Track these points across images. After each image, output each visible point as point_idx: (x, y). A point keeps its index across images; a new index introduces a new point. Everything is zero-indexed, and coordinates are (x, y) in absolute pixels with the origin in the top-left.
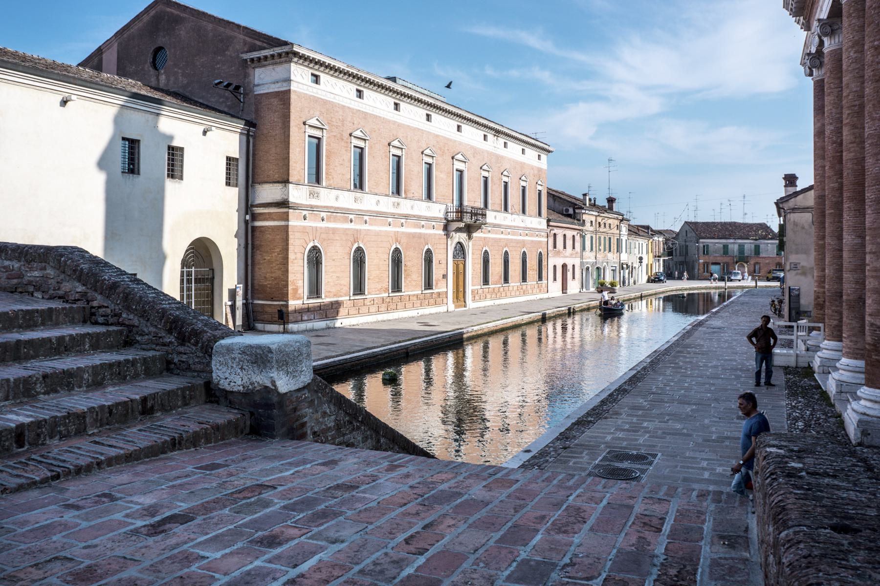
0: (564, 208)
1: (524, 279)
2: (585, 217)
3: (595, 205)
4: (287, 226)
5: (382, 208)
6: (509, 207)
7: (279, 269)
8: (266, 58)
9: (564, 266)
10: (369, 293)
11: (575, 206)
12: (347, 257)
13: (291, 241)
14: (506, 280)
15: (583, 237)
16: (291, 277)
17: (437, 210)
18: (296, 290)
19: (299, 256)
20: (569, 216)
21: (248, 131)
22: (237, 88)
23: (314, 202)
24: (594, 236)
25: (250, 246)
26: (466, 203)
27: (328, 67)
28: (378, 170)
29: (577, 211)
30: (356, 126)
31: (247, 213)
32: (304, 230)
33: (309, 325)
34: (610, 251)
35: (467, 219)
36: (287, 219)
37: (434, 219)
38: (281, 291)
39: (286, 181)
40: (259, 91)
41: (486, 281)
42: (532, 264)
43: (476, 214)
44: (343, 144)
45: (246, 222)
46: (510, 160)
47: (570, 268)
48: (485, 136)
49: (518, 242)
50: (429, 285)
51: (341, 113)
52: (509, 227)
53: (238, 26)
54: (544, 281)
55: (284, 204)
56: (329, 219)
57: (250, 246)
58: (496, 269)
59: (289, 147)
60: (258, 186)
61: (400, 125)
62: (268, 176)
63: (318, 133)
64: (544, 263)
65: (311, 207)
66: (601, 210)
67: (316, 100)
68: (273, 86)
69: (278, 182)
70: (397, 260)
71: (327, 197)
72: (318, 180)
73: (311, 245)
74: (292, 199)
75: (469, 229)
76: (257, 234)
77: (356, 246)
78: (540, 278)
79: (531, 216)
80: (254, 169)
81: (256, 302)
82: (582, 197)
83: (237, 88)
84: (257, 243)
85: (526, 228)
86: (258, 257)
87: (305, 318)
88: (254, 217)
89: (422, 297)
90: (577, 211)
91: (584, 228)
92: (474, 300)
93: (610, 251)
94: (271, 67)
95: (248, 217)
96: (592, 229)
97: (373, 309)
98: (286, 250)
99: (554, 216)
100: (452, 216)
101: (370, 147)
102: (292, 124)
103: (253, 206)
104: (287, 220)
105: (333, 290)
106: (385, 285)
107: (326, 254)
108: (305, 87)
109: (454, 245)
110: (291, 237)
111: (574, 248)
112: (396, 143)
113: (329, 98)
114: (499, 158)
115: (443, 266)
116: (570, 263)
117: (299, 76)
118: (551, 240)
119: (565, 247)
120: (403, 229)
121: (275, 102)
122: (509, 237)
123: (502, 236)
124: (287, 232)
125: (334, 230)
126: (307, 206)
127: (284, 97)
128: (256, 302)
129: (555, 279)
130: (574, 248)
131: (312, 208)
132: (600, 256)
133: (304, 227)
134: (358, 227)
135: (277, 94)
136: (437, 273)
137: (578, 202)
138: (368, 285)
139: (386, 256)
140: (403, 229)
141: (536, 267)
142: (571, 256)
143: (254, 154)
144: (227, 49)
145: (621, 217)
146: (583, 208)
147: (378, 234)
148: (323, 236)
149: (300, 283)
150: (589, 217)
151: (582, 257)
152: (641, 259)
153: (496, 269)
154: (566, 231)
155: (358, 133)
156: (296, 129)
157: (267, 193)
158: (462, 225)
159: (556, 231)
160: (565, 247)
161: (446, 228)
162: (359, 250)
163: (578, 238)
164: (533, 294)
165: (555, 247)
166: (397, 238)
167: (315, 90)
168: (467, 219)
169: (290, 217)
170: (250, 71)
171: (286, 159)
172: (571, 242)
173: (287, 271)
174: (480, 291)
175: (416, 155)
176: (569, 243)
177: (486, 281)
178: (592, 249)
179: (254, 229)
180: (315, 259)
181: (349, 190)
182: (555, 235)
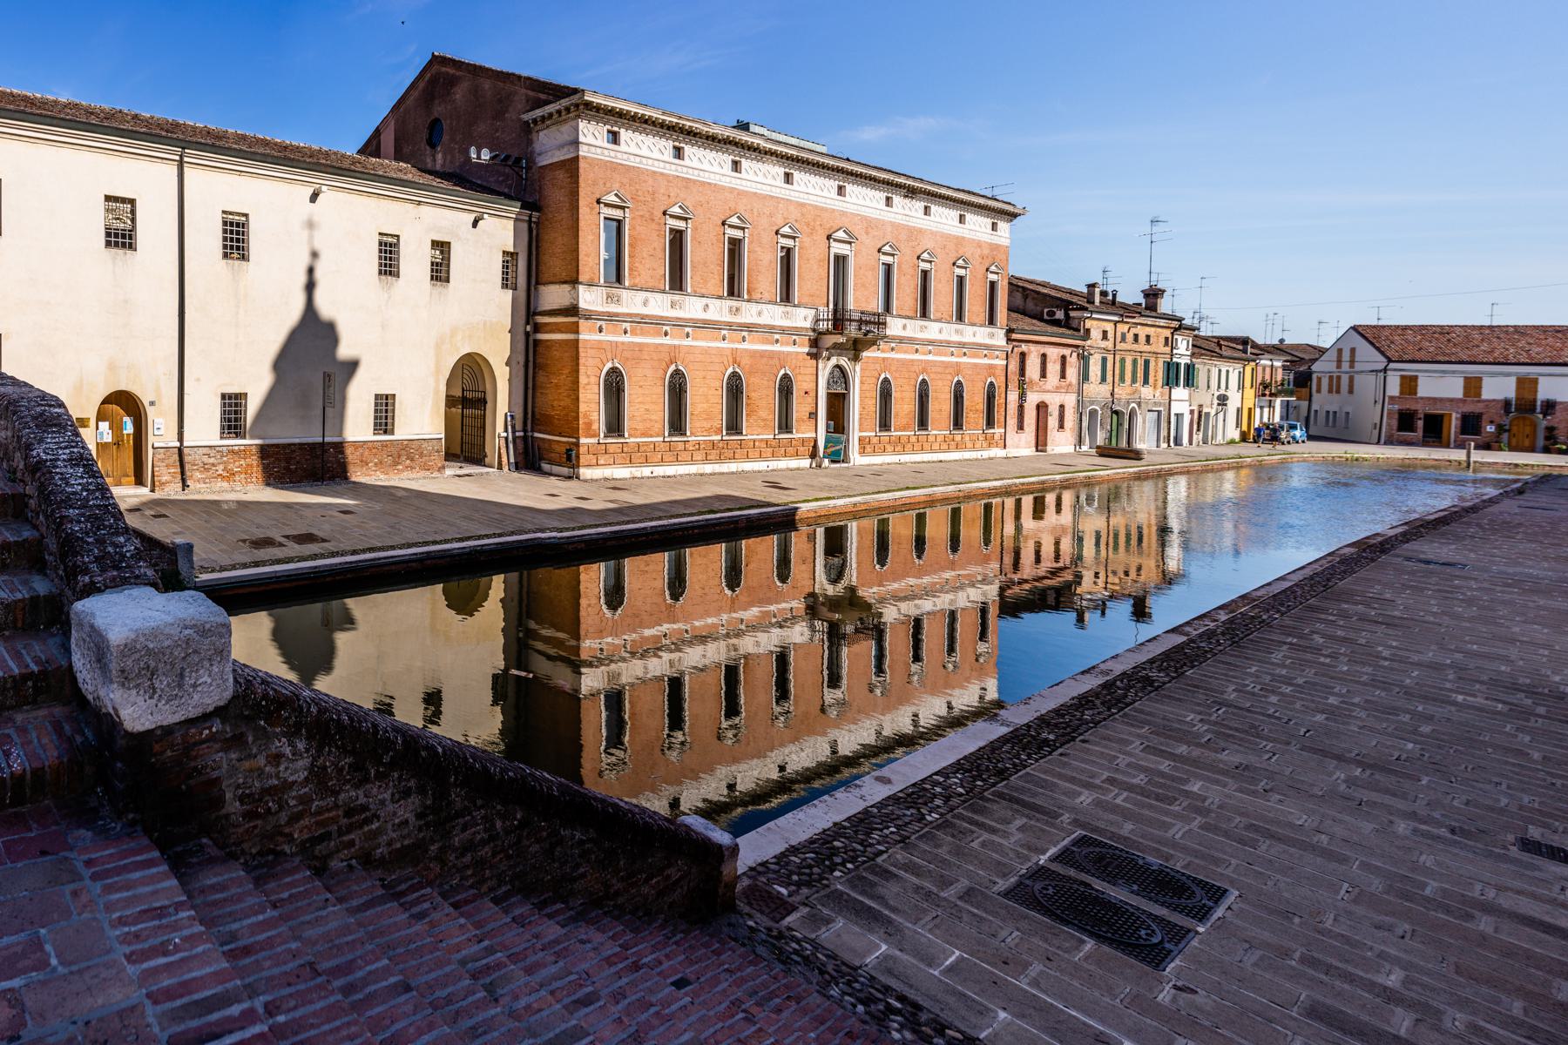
0: (1044, 309)
3: (1114, 302)
4: (577, 341)
5: (712, 315)
6: (932, 307)
9: (1042, 408)
11: (1066, 305)
12: (660, 383)
13: (582, 361)
15: (1084, 359)
16: (583, 408)
17: (801, 318)
19: (593, 380)
22: (518, 160)
24: (1110, 358)
28: (704, 257)
29: (1072, 314)
30: (673, 200)
32: (599, 346)
35: (852, 330)
36: (575, 329)
37: (796, 331)
39: (574, 281)
40: (544, 161)
43: (867, 323)
44: (654, 226)
45: (527, 334)
46: (932, 233)
51: (650, 182)
54: (998, 431)
56: (634, 333)
59: (577, 236)
60: (542, 288)
61: (741, 194)
63: (617, 214)
66: (1127, 311)
67: (614, 167)
68: (557, 153)
71: (632, 302)
73: (609, 365)
74: (582, 305)
75: (855, 348)
76: (540, 349)
77: (673, 368)
79: (973, 325)
80: (539, 264)
82: (1085, 290)
83: (518, 160)
84: (539, 360)
85: (962, 345)
86: (541, 378)
88: (537, 328)
89: (774, 443)
90: (1072, 314)
91: (1089, 342)
96: (1109, 344)
100: (823, 326)
101: (695, 229)
102: (582, 203)
103: (536, 314)
105: (640, 426)
106: (717, 424)
110: (582, 354)
111: (1063, 376)
113: (633, 162)
115: (810, 399)
116: (1053, 401)
117: (591, 135)
118: (1014, 366)
119: (1043, 375)
120: (745, 346)
121: (561, 175)
124: (577, 348)
126: (603, 313)
127: (571, 166)
130: (1063, 376)
131: (611, 317)
132: (1123, 392)
134: (676, 342)
137: (1075, 299)
138: (689, 424)
142: (1057, 390)
145: (1175, 324)
148: (626, 354)
149: (594, 416)
150: (1096, 326)
151: (1080, 392)
154: (1043, 350)
155: (676, 210)
157: (553, 296)
158: (841, 339)
159: (1024, 347)
160: (1043, 375)
161: (814, 343)
162: (677, 373)
166: (735, 358)
168: (852, 330)
171: (575, 251)
172: (1058, 367)
174: (875, 440)
176: (1053, 368)
181: (663, 292)
182: (1023, 355)
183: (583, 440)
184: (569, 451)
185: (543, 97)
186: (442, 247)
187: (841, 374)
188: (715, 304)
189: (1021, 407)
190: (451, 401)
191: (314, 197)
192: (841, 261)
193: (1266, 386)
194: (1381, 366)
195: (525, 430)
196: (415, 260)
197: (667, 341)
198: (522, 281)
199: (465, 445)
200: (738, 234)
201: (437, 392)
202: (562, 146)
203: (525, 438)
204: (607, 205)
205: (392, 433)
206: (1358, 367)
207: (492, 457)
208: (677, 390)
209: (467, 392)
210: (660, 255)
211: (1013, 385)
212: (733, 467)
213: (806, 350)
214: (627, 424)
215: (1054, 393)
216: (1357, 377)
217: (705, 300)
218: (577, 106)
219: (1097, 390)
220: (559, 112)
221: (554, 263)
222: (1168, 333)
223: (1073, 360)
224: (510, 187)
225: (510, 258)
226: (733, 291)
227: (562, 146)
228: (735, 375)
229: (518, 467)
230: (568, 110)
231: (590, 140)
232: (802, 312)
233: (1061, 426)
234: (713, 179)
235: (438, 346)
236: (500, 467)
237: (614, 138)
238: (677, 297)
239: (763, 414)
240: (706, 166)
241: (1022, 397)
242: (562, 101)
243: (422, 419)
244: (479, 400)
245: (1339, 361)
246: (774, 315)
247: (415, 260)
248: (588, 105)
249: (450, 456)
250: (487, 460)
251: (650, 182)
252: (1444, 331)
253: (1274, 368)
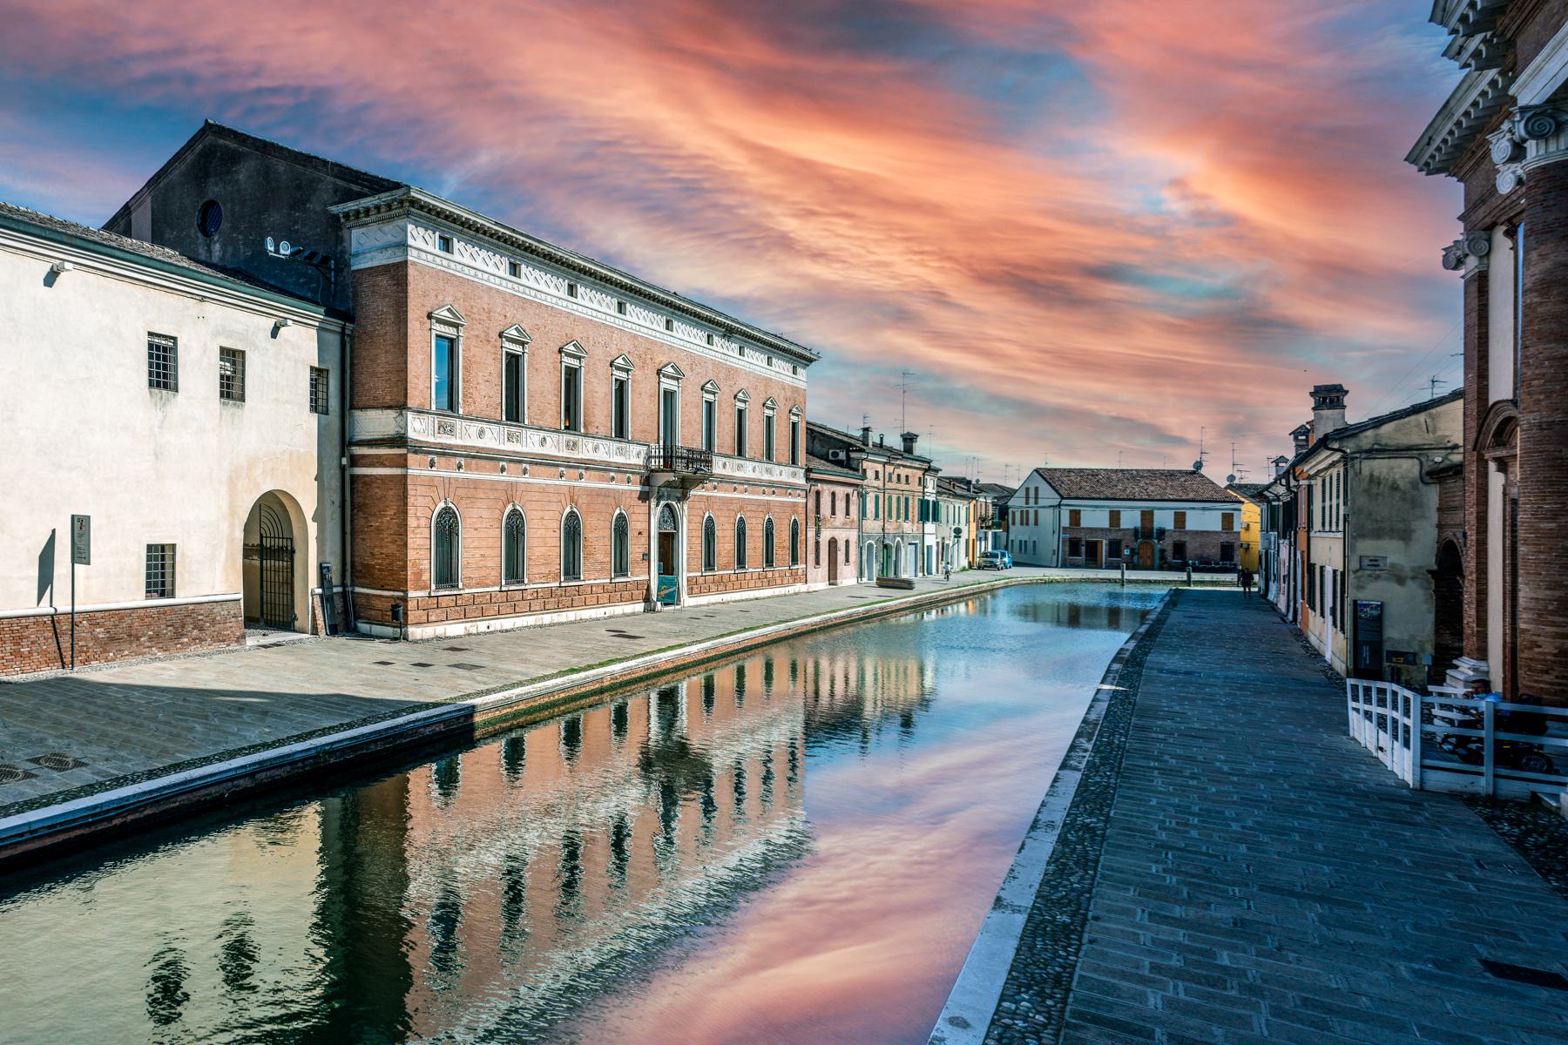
0: (832, 452)
1: (769, 561)
2: (865, 464)
3: (881, 445)
4: (405, 476)
5: (550, 450)
7: (394, 542)
8: (367, 211)
9: (833, 543)
11: (847, 447)
12: (496, 525)
13: (411, 500)
14: (741, 562)
15: (862, 496)
16: (411, 555)
17: (634, 456)
18: (419, 574)
19: (423, 522)
20: (839, 463)
21: (343, 328)
22: (325, 260)
23: (445, 439)
25: (348, 504)
27: (466, 224)
28: (541, 387)
29: (853, 455)
31: (343, 455)
32: (431, 483)
33: (439, 630)
34: (907, 518)
36: (402, 463)
38: (396, 577)
39: (401, 406)
41: (709, 565)
42: (782, 537)
43: (697, 460)
44: (489, 348)
45: (343, 469)
47: (841, 546)
49: (759, 503)
50: (621, 568)
51: (486, 299)
52: (747, 482)
53: (325, 163)
55: (400, 440)
56: (469, 468)
57: (348, 504)
58: (725, 545)
60: (358, 413)
61: (578, 319)
62: (376, 398)
63: (450, 331)
64: (801, 537)
65: (442, 446)
66: (890, 455)
68: (380, 256)
69: (390, 407)
70: (572, 531)
72: (452, 405)
73: (442, 505)
74: (411, 434)
76: (359, 486)
77: (510, 508)
78: (795, 560)
81: (358, 590)
83: (325, 260)
85: (771, 484)
87: (433, 618)
89: (610, 587)
90: (853, 455)
93: (907, 518)
94: (374, 227)
95: (344, 461)
96: (879, 483)
97: (536, 605)
98: (403, 512)
99: (816, 463)
103: (352, 444)
104: (405, 466)
108: (430, 257)
109: (659, 509)
110: (411, 492)
111: (848, 513)
112: (570, 348)
113: (468, 274)
114: (731, 372)
115: (644, 540)
119: (833, 513)
120: (582, 483)
121: (384, 281)
122: (746, 496)
123: (736, 495)
125: (476, 484)
127: (398, 273)
128: (358, 590)
129: (818, 563)
130: (848, 513)
133: (432, 478)
135: (385, 269)
136: (635, 549)
139: (555, 525)
140: (582, 483)
141: (788, 543)
142: (844, 526)
143: (352, 365)
144: (308, 201)
145: (925, 466)
146: (862, 451)
147: (543, 490)
148: (461, 492)
151: (860, 528)
152: (958, 532)
153: (725, 545)
155: (513, 332)
156: (417, 325)
157: (374, 423)
158: (671, 477)
160: (833, 513)
161: (646, 481)
163: (854, 499)
164: (782, 585)
165: (818, 511)
167: (445, 263)
168: (679, 466)
169: (410, 462)
170: (345, 232)
171: (402, 371)
172: (844, 504)
173: (406, 545)
174: (701, 580)
175: (603, 368)
176: (841, 505)
177: (709, 565)
178: (877, 516)
179: (352, 476)
180: (447, 530)
181: (499, 423)
182: (818, 493)
183: (411, 594)
184: (395, 606)
185: (356, 188)
186: (234, 357)
187: (671, 515)
188: (552, 438)
189: (817, 543)
190: (248, 551)
191: (51, 278)
192: (669, 396)
193: (984, 520)
194: (1056, 502)
195: (343, 585)
196: (198, 370)
197: (504, 477)
198: (334, 403)
199: (267, 608)
200: (574, 363)
201: (231, 540)
202: (385, 248)
203: (344, 594)
204: (440, 321)
205: (173, 595)
206: (1041, 502)
207: (303, 619)
208: (515, 531)
209: (268, 540)
210: (497, 381)
211: (811, 522)
212: (571, 616)
213: (639, 488)
214: (462, 573)
215: (839, 529)
216: (1041, 511)
217: (542, 434)
218: (401, 202)
219: (872, 526)
220: (378, 208)
221: (375, 383)
222: (920, 473)
223: (854, 499)
224: (314, 291)
225: (318, 374)
226: (572, 424)
227: (385, 248)
228: (572, 515)
229: (333, 630)
230: (389, 207)
231: (420, 244)
232: (635, 448)
233: (847, 560)
234: (550, 301)
235: (232, 482)
236: (315, 631)
237: (446, 245)
238: (513, 429)
239: (600, 557)
240: (542, 287)
241: (818, 533)
242: (388, 197)
243: (213, 576)
244: (281, 549)
245: (1027, 498)
246: (607, 451)
247: (198, 370)
248: (414, 202)
249: (251, 622)
250: (297, 624)
251: (486, 299)
252: (1094, 473)
253: (986, 502)
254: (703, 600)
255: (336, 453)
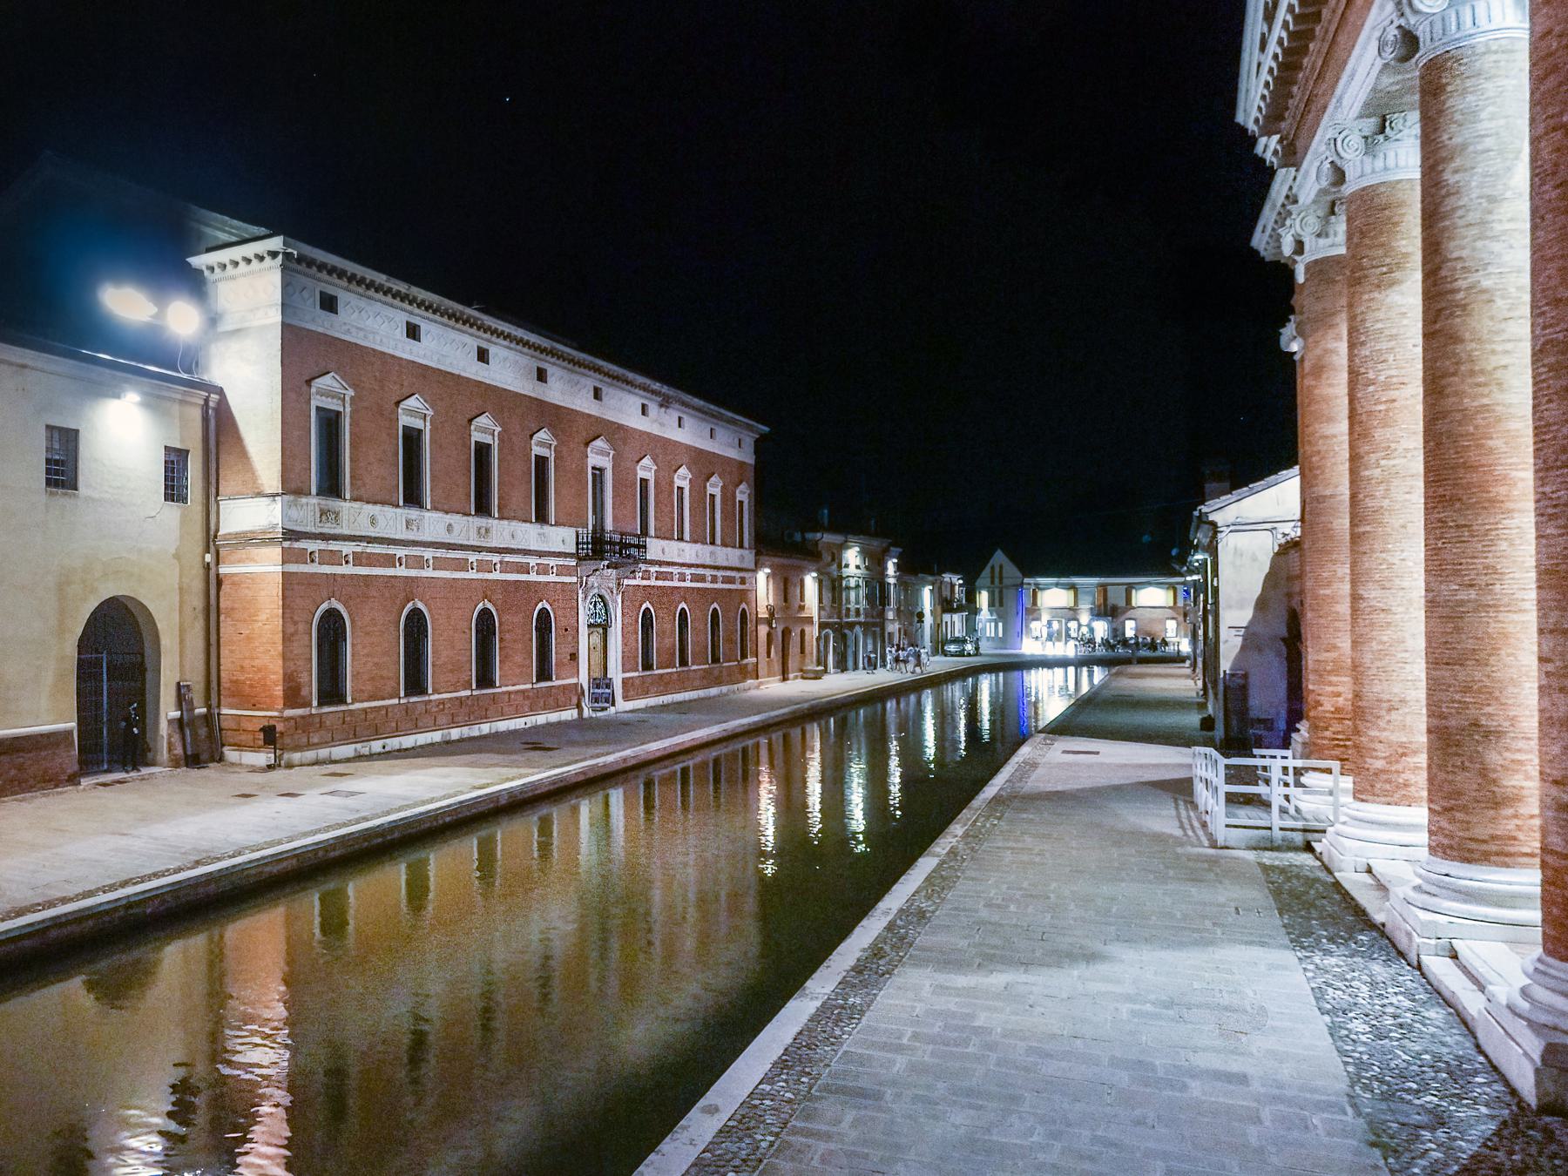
10: (435, 691)
19: (301, 627)
26: (609, 525)
45: (207, 567)
48: (644, 406)
50: (544, 674)
77: (410, 606)
92: (626, 698)
95: (208, 558)
97: (442, 719)
107: (353, 622)
162: (416, 615)
239: (518, 659)
254: (641, 703)
255: (199, 549)
